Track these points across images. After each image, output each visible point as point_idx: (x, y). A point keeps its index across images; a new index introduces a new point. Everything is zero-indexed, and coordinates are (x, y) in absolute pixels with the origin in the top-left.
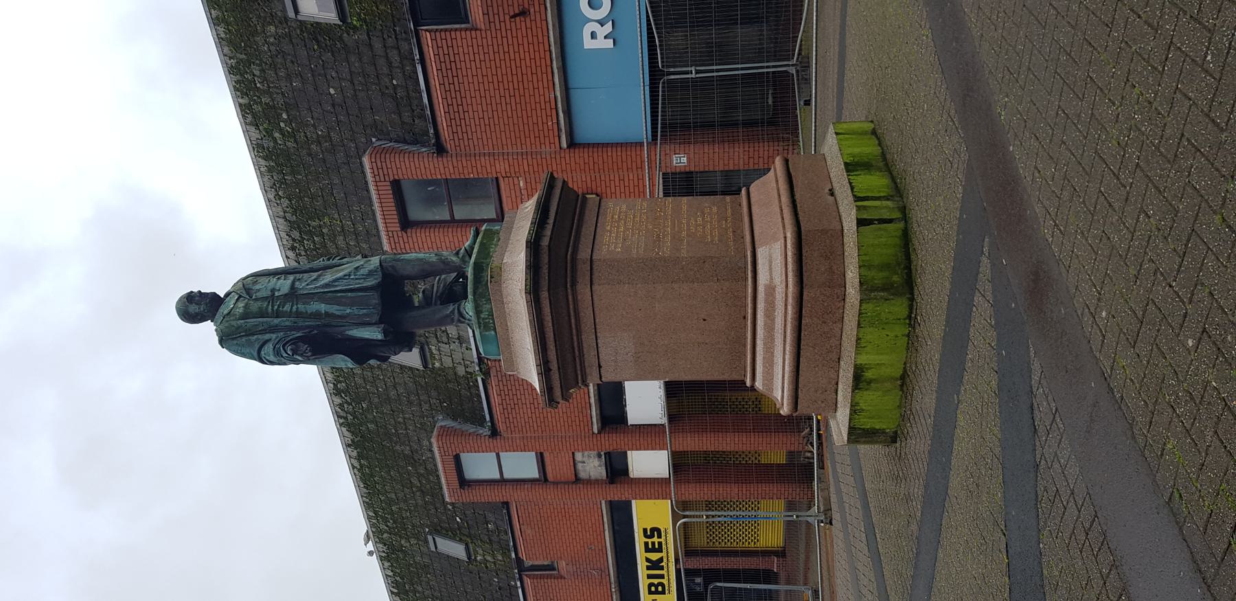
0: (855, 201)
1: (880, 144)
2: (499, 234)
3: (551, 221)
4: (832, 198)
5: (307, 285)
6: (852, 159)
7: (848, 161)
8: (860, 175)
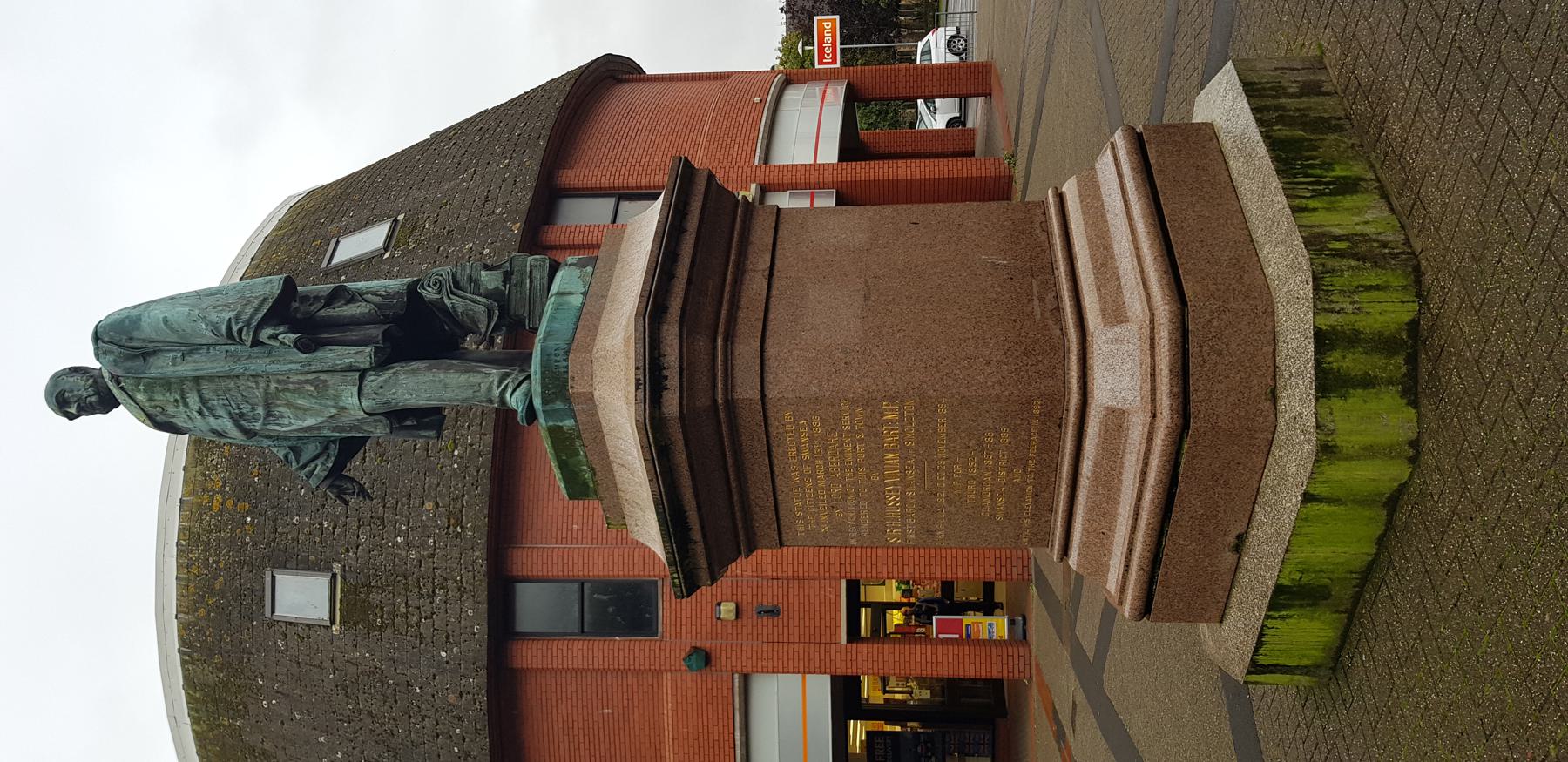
0: (1249, 673)
1: (1381, 542)
2: (579, 437)
3: (697, 534)
4: (1230, 558)
5: (264, 424)
6: (1297, 576)
7: (1286, 582)
8: (1291, 617)
